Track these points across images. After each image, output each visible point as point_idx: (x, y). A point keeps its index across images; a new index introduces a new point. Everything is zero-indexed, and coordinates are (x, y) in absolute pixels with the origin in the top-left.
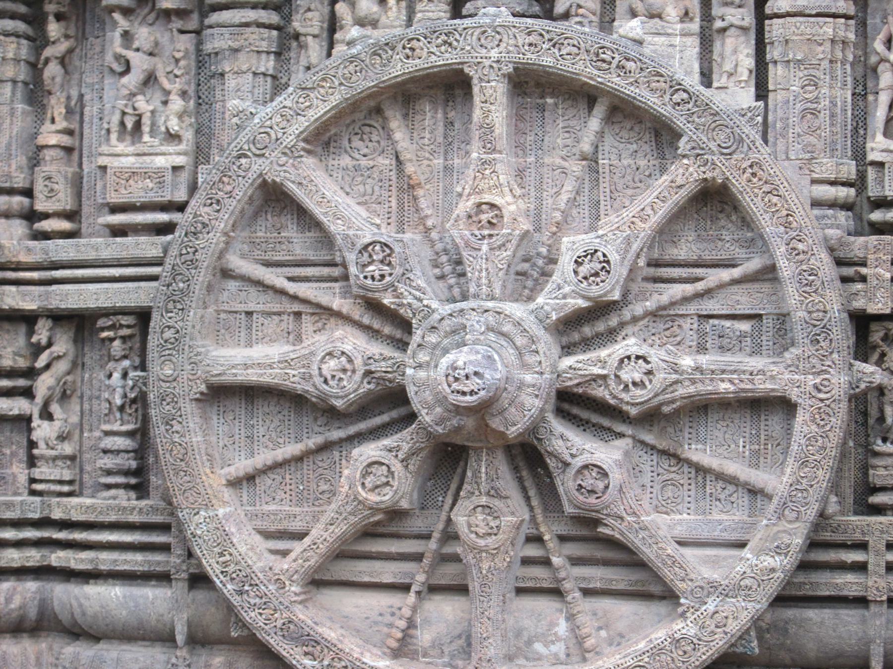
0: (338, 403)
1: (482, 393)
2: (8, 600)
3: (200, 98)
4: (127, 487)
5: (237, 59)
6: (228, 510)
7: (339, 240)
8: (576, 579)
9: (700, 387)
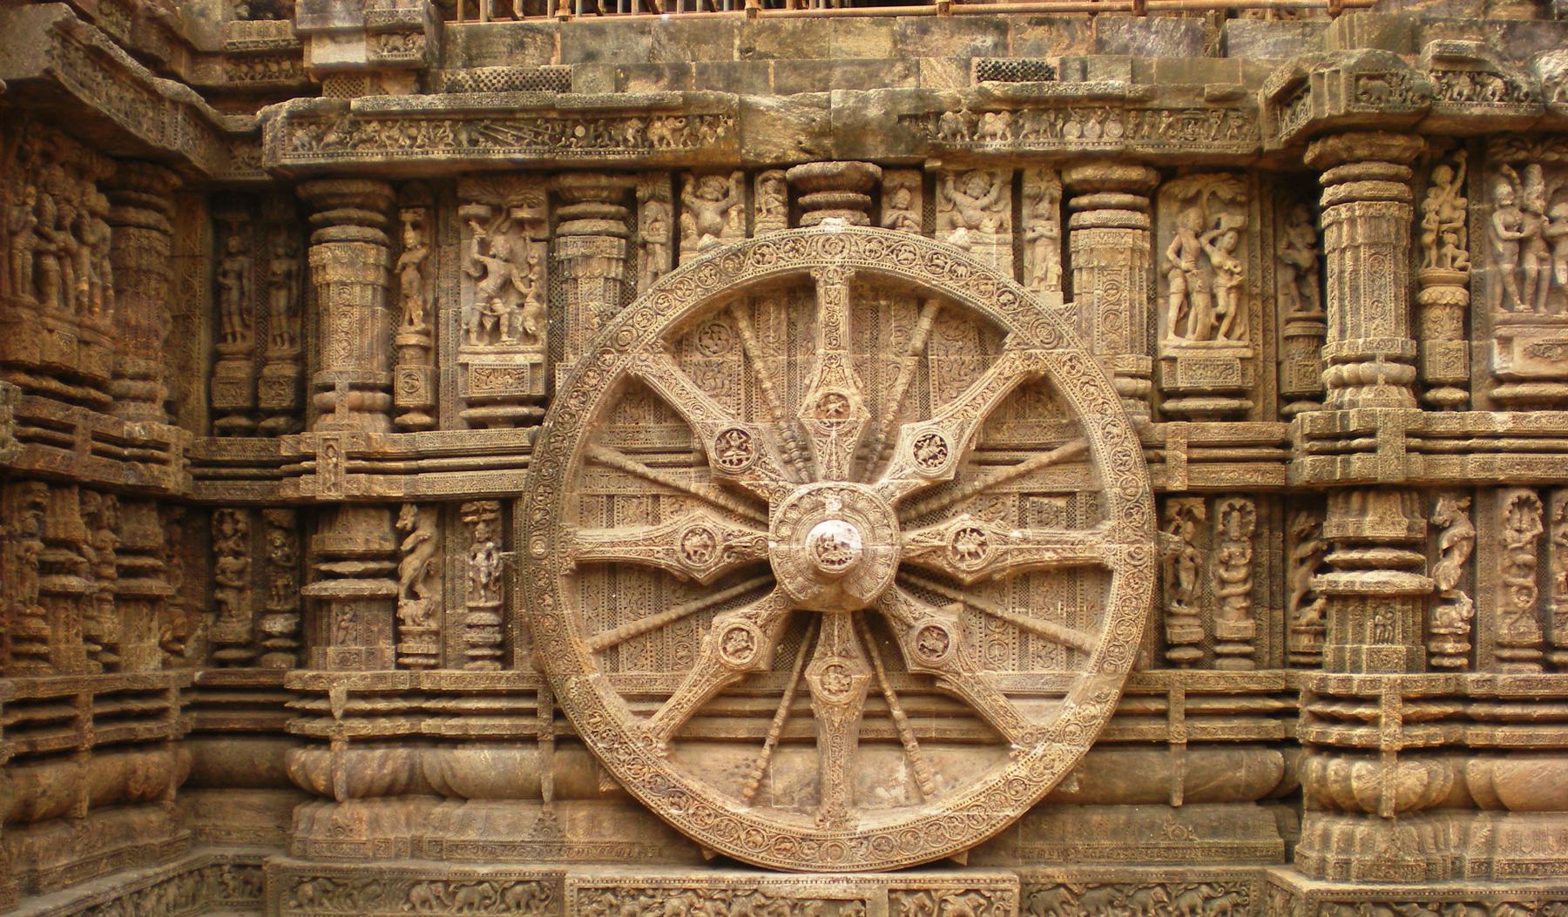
0: (700, 576)
1: (849, 562)
2: (382, 765)
3: (550, 301)
4: (493, 658)
5: (589, 266)
6: (597, 675)
7: (698, 428)
8: (913, 730)
9: (1028, 556)
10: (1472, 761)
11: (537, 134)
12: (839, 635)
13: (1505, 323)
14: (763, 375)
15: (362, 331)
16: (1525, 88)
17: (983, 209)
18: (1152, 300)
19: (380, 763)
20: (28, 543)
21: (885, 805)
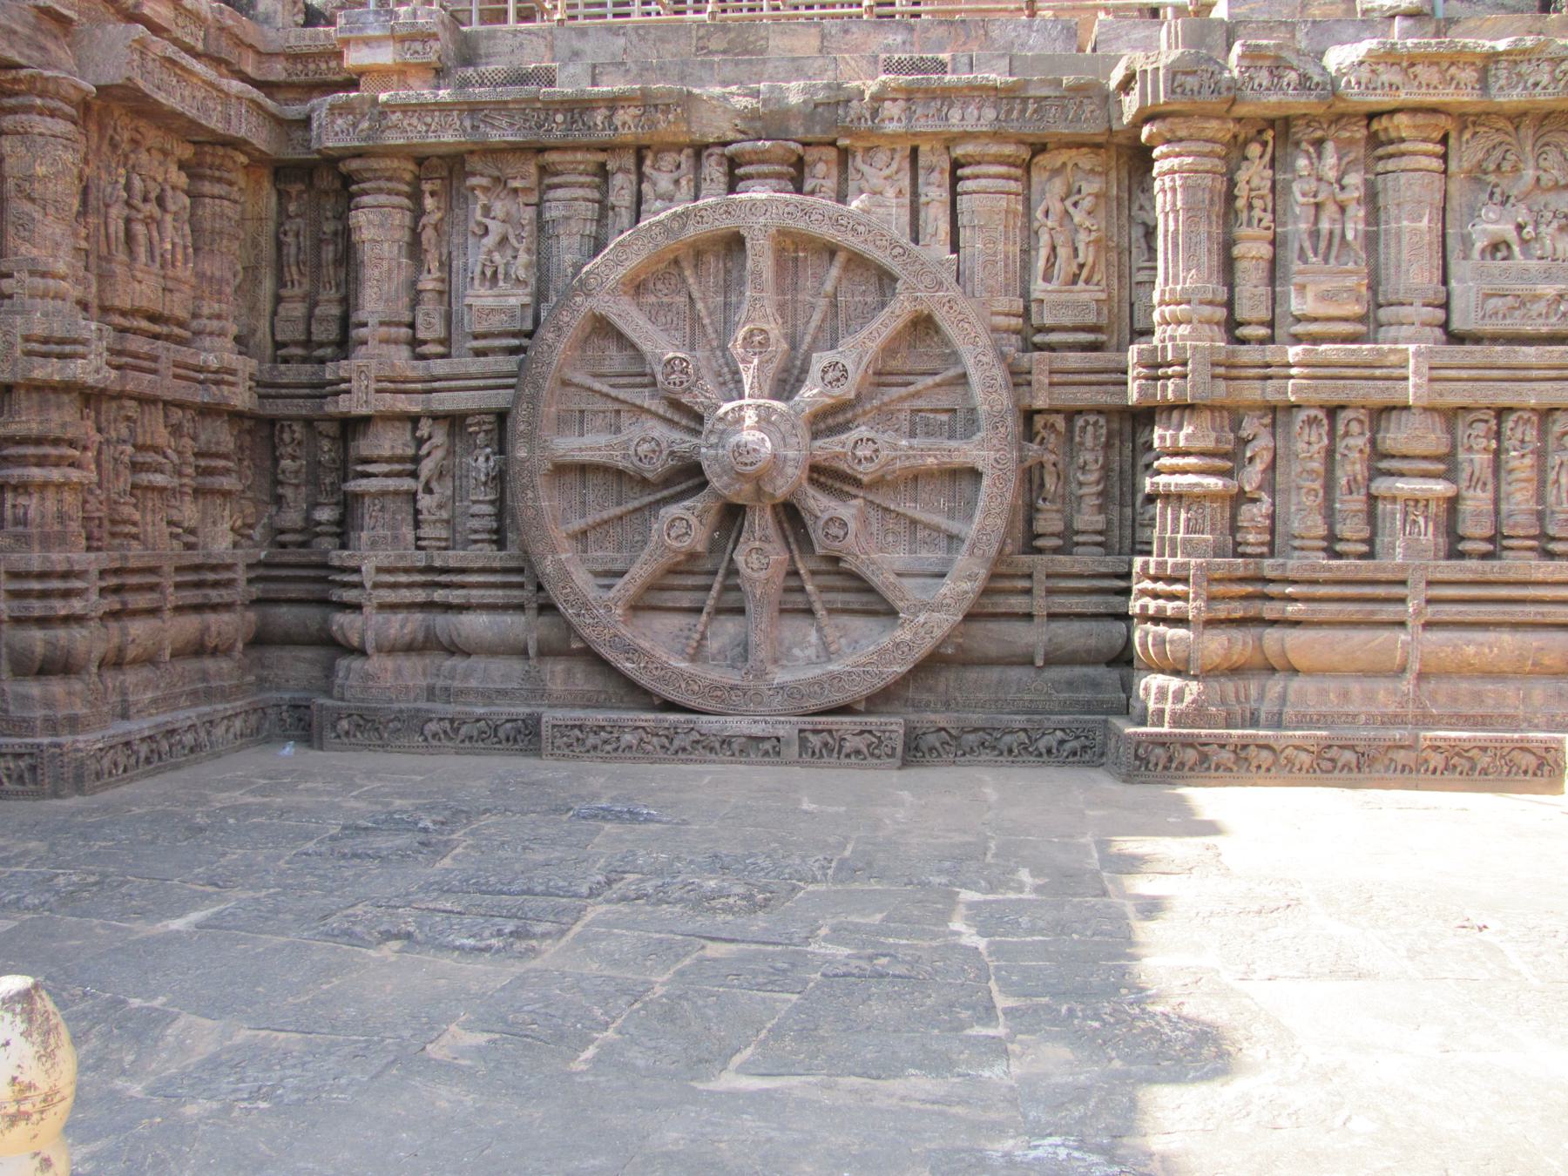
0: (648, 475)
2: (402, 627)
9: (913, 461)
10: (1269, 630)
11: (526, 120)
12: (761, 523)
13: (1300, 273)
14: (703, 313)
15: (390, 278)
16: (1316, 79)
17: (886, 178)
20: (121, 448)
21: (801, 663)
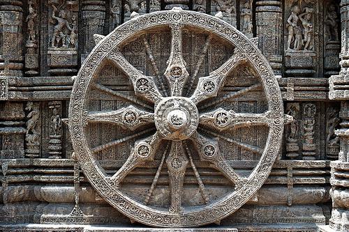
4: (59, 155)
12: (176, 148)
14: (153, 60)
18: (282, 36)
19: (18, 192)
